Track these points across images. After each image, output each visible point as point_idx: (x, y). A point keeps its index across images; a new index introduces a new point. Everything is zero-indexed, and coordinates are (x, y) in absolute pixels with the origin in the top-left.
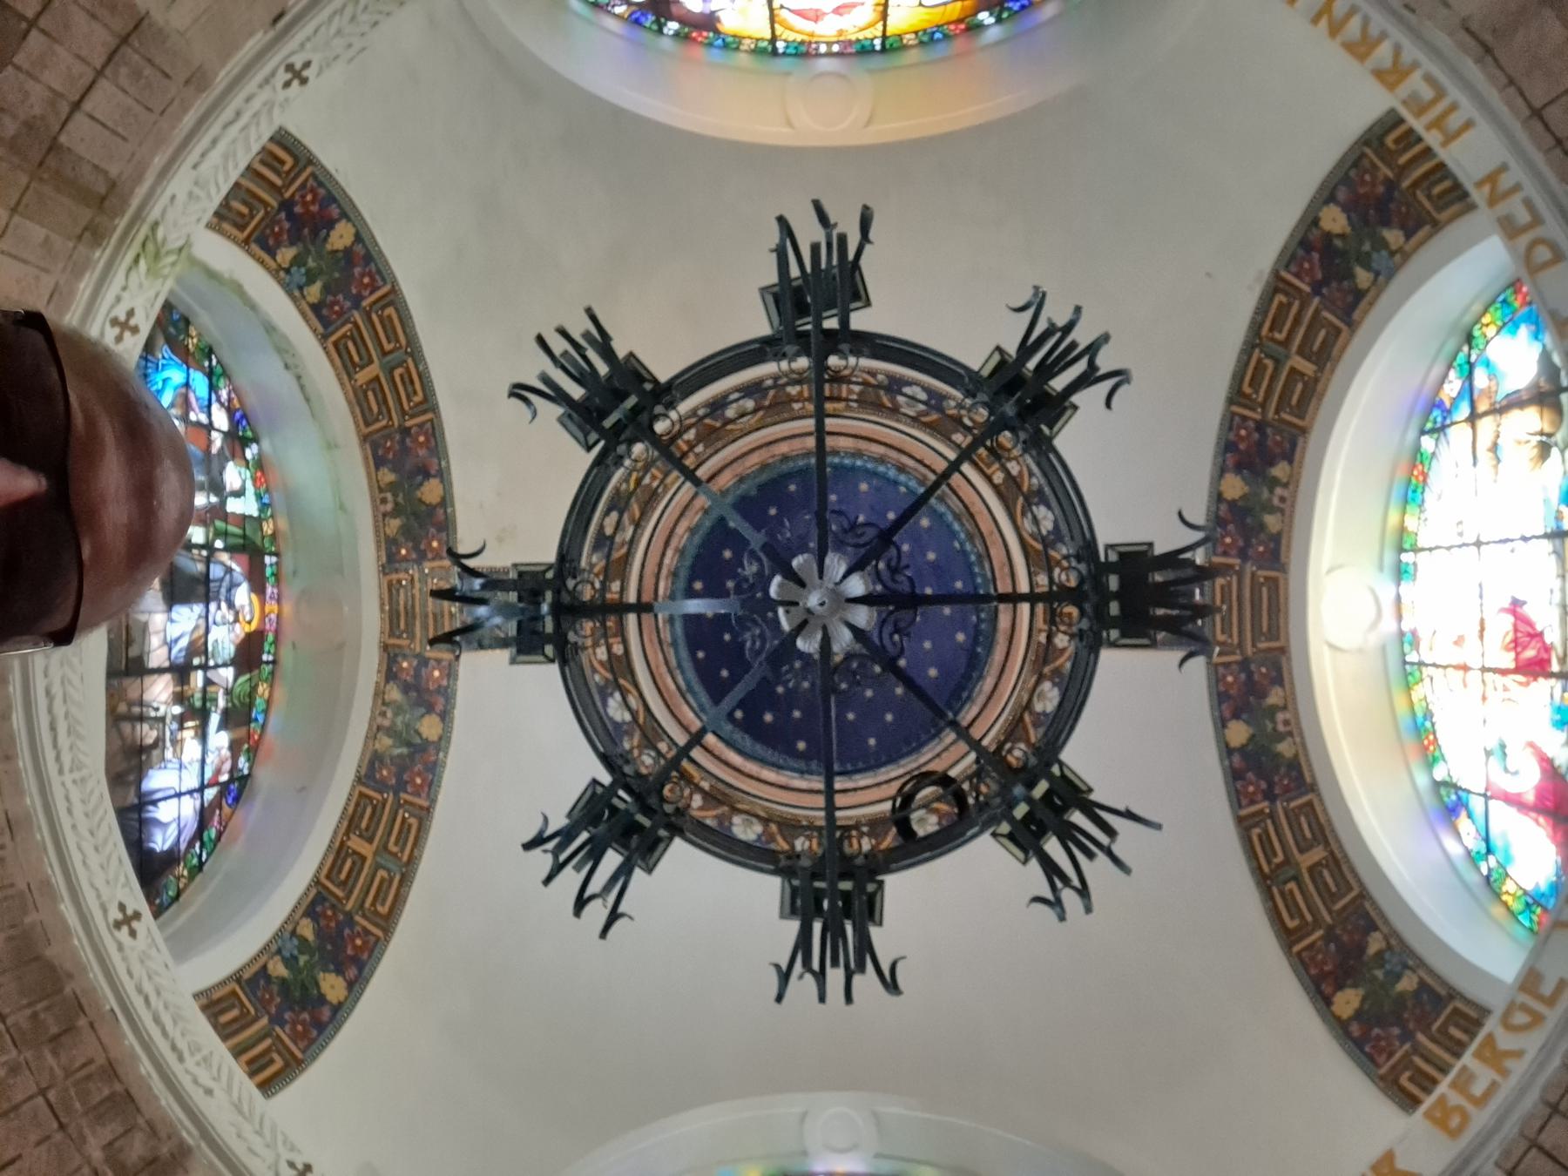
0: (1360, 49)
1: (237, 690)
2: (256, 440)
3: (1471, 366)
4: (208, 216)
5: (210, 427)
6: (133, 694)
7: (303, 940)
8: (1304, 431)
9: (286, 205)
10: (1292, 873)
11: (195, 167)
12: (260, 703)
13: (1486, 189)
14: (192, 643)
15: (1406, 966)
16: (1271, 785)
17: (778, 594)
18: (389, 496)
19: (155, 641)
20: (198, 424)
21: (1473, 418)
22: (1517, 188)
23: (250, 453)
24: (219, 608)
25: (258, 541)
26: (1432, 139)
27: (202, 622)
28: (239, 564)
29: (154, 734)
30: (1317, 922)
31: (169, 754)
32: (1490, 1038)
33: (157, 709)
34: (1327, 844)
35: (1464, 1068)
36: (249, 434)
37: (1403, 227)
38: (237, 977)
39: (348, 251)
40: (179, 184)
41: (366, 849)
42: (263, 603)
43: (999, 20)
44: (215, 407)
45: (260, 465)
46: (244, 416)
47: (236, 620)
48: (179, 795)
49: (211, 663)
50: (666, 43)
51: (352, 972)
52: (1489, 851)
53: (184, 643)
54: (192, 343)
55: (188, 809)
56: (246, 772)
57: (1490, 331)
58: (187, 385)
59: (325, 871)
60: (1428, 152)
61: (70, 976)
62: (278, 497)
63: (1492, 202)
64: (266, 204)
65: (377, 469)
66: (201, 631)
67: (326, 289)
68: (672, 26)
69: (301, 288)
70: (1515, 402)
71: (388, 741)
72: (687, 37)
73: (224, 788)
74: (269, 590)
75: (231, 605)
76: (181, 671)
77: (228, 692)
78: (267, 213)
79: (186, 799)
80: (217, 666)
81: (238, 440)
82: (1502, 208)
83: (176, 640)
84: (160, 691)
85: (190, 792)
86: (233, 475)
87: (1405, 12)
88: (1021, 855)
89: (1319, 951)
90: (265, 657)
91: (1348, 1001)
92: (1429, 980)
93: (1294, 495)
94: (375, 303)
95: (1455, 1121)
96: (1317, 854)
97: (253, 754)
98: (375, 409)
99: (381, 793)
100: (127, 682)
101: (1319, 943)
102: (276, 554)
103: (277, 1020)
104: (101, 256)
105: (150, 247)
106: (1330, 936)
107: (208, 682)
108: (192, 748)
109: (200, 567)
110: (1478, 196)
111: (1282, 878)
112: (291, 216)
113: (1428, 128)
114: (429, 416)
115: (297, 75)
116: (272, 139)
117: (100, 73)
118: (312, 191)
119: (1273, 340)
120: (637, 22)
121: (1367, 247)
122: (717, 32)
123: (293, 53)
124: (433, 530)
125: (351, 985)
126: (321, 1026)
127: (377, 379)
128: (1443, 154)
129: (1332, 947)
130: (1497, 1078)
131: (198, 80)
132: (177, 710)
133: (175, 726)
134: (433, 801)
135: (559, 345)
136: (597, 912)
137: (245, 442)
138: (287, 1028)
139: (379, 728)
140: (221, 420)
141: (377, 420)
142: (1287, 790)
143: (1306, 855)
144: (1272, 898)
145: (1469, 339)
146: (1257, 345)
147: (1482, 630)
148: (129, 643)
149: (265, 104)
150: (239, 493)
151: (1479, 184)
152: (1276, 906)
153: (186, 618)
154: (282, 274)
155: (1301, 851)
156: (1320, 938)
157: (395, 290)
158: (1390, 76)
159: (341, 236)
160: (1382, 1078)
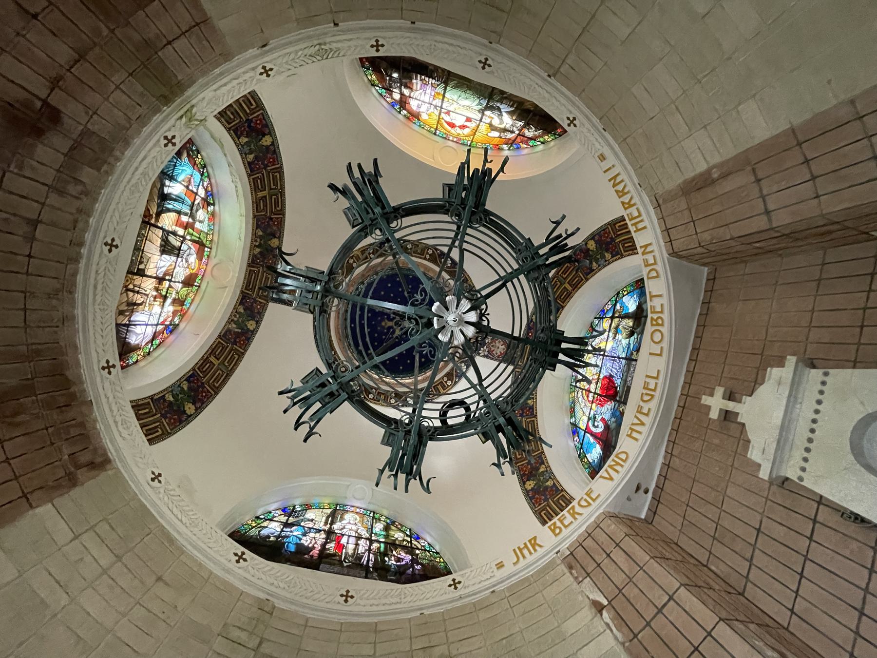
0: (621, 194)
1: (181, 293)
2: (214, 204)
3: (616, 302)
4: (216, 112)
5: (196, 194)
6: (137, 282)
7: (182, 388)
9: (249, 121)
11: (215, 90)
12: (189, 300)
13: (643, 249)
14: (167, 270)
15: (550, 478)
16: (523, 412)
17: (436, 311)
18: (258, 240)
19: (151, 265)
20: (192, 191)
21: (612, 318)
22: (652, 252)
23: (210, 208)
24: (182, 261)
25: (204, 241)
26: (632, 229)
27: (174, 264)
28: (195, 247)
29: (142, 300)
31: (147, 309)
32: (573, 508)
33: (146, 291)
35: (563, 515)
36: (212, 202)
37: (611, 253)
38: (152, 397)
39: (267, 147)
40: (208, 94)
41: (216, 362)
42: (200, 264)
43: (509, 149)
44: (201, 187)
45: (213, 215)
46: (212, 195)
47: (188, 267)
48: (147, 325)
49: (173, 280)
50: (401, 117)
51: (198, 405)
52: (581, 448)
53: (164, 269)
54: (198, 161)
55: (150, 331)
56: (177, 323)
57: (625, 293)
58: (191, 176)
59: (198, 366)
60: (629, 232)
61: (74, 383)
62: (216, 228)
63: (643, 253)
64: (241, 118)
65: (257, 229)
66: (173, 267)
67: (256, 158)
68: (404, 112)
69: (246, 154)
70: (627, 316)
71: (234, 326)
72: (408, 118)
73: (167, 327)
74: (204, 260)
75: (187, 261)
76: (160, 280)
77: (177, 293)
78: (240, 121)
79: (149, 327)
80: (175, 282)
81: (207, 202)
82: (646, 257)
83: (161, 268)
84: (148, 285)
85: (152, 325)
86: (201, 214)
87: (638, 186)
88: (483, 440)
90: (196, 284)
94: (273, 169)
95: (557, 531)
97: (182, 316)
98: (262, 208)
99: (227, 343)
100: (135, 277)
102: (211, 249)
103: (164, 416)
104: (166, 110)
105: (189, 114)
107: (170, 286)
108: (157, 309)
109: (179, 244)
110: (640, 250)
112: (249, 126)
113: (632, 225)
114: (281, 216)
115: (266, 72)
116: (249, 93)
117: (183, 33)
118: (260, 120)
120: (393, 106)
121: (599, 257)
122: (419, 120)
123: (267, 62)
124: (271, 257)
125: (196, 409)
126: (181, 422)
127: (265, 197)
128: (633, 234)
129: (529, 466)
130: (573, 520)
131: (227, 56)
132: (155, 293)
133: (152, 299)
134: (246, 351)
135: (357, 174)
136: (304, 429)
137: (209, 204)
138: (167, 420)
139: (232, 320)
140: (202, 193)
141: (261, 212)
142: (527, 415)
145: (618, 294)
148: (141, 263)
149: (250, 77)
150: (200, 222)
151: (641, 247)
153: (167, 260)
154: (240, 147)
157: (281, 167)
158: (627, 205)
159: (267, 141)
160: (536, 511)
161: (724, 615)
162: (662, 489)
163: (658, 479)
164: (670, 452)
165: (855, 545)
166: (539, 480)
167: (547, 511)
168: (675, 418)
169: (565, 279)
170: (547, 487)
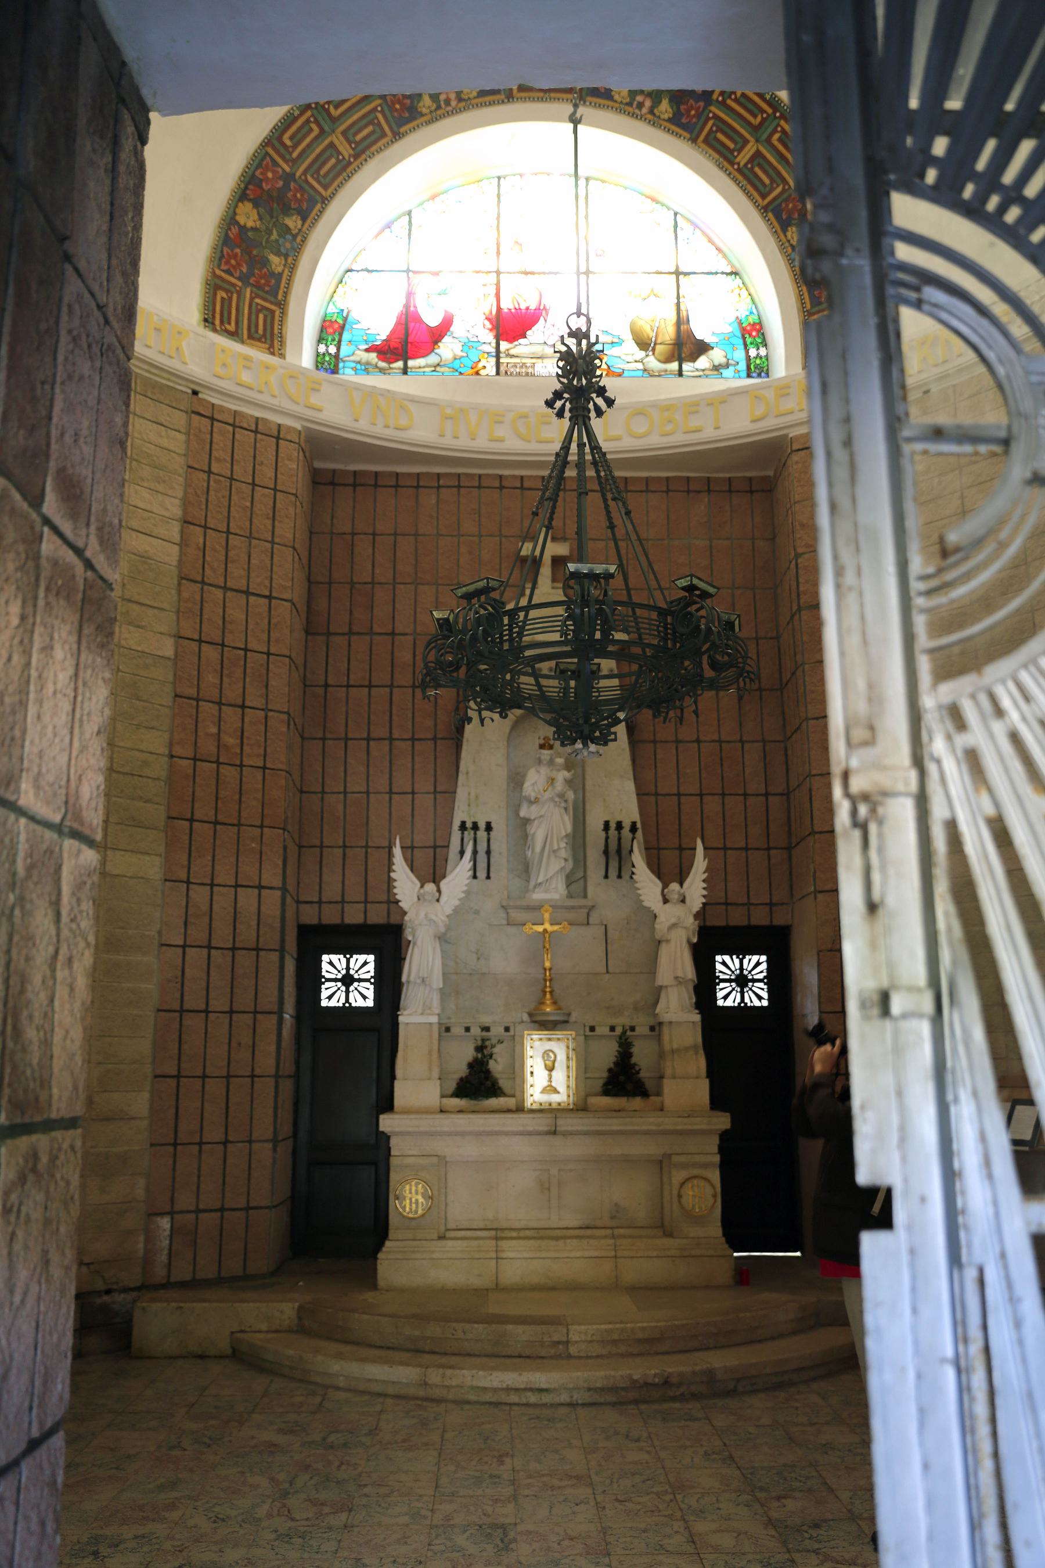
8: (694, 140)
10: (326, 128)
15: (286, 256)
30: (294, 162)
34: (356, 157)
89: (274, 172)
91: (248, 216)
92: (284, 280)
93: (641, 118)
96: (346, 150)
101: (280, 170)
106: (289, 177)
111: (320, 119)
119: (775, 131)
143: (342, 138)
144: (302, 113)
145: (735, 273)
146: (774, 113)
147: (526, 273)
152: (296, 119)
155: (344, 133)
156: (283, 170)
161: (293, 656)
162: (376, 485)
163: (391, 474)
164: (442, 482)
165: (430, 723)
166: (269, 232)
167: (230, 299)
168: (501, 477)
169: (768, 141)
170: (266, 262)
